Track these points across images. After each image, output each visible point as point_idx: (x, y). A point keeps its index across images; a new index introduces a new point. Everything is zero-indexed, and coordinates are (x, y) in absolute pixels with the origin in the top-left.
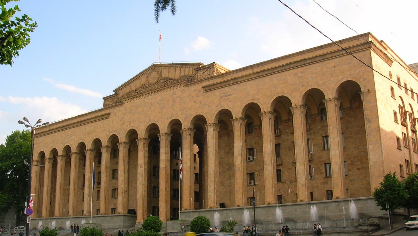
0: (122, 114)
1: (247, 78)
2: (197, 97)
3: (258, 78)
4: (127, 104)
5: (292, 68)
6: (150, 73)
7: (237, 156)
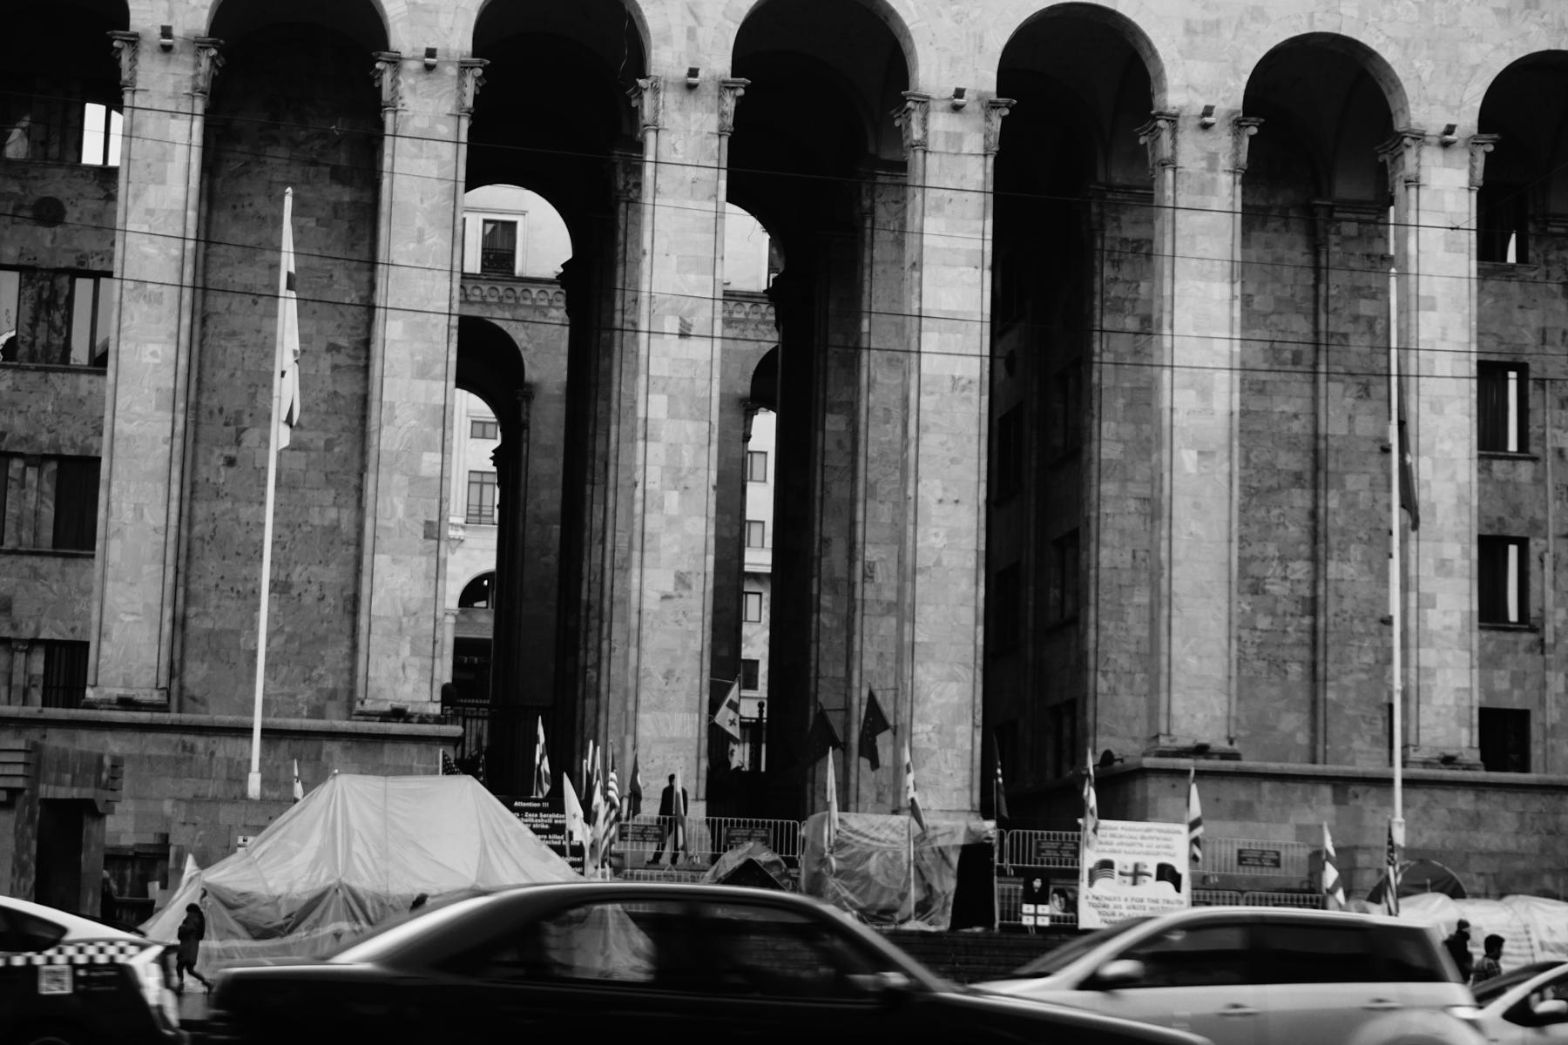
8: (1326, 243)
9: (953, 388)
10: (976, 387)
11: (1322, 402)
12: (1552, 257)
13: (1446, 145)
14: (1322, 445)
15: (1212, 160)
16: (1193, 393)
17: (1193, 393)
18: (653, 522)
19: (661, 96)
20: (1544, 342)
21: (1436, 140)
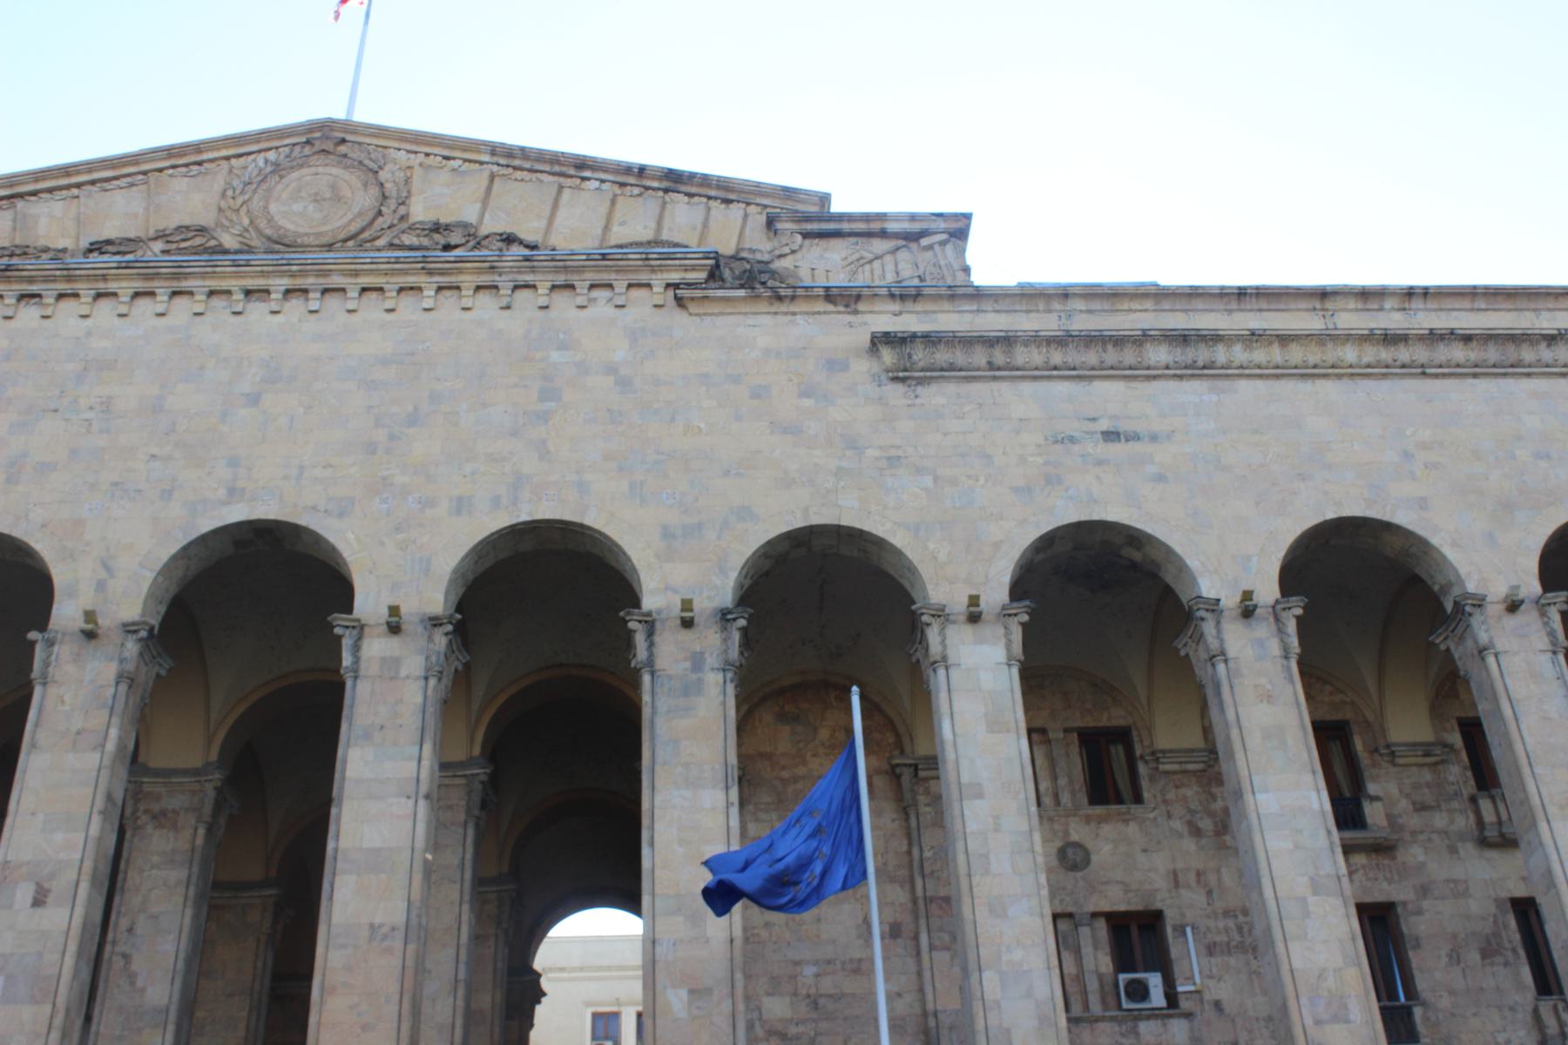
1: (1296, 354)
2: (807, 402)
3: (1383, 372)
6: (278, 169)
7: (1303, 900)
8: (915, 805)
9: (371, 938)
10: (399, 936)
11: (927, 975)
12: (1171, 795)
13: (974, 618)
14: (932, 1022)
15: (697, 662)
16: (680, 919)
17: (680, 919)
19: (56, 648)
20: (1177, 884)
21: (963, 618)
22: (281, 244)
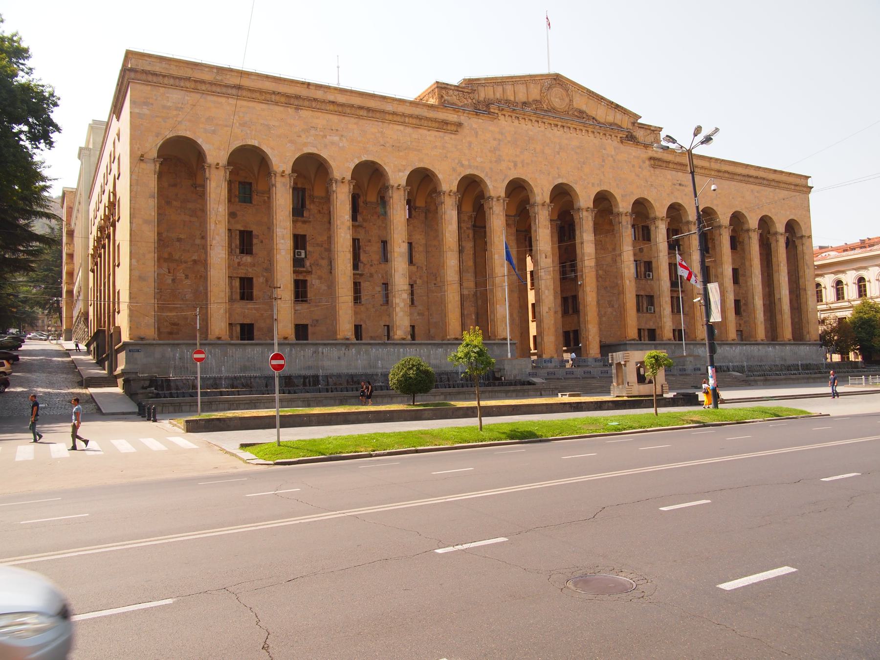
0: (495, 139)
4: (505, 124)
5: (751, 183)
18: (543, 297)
22: (553, 110)
